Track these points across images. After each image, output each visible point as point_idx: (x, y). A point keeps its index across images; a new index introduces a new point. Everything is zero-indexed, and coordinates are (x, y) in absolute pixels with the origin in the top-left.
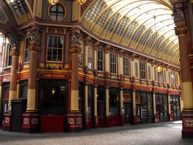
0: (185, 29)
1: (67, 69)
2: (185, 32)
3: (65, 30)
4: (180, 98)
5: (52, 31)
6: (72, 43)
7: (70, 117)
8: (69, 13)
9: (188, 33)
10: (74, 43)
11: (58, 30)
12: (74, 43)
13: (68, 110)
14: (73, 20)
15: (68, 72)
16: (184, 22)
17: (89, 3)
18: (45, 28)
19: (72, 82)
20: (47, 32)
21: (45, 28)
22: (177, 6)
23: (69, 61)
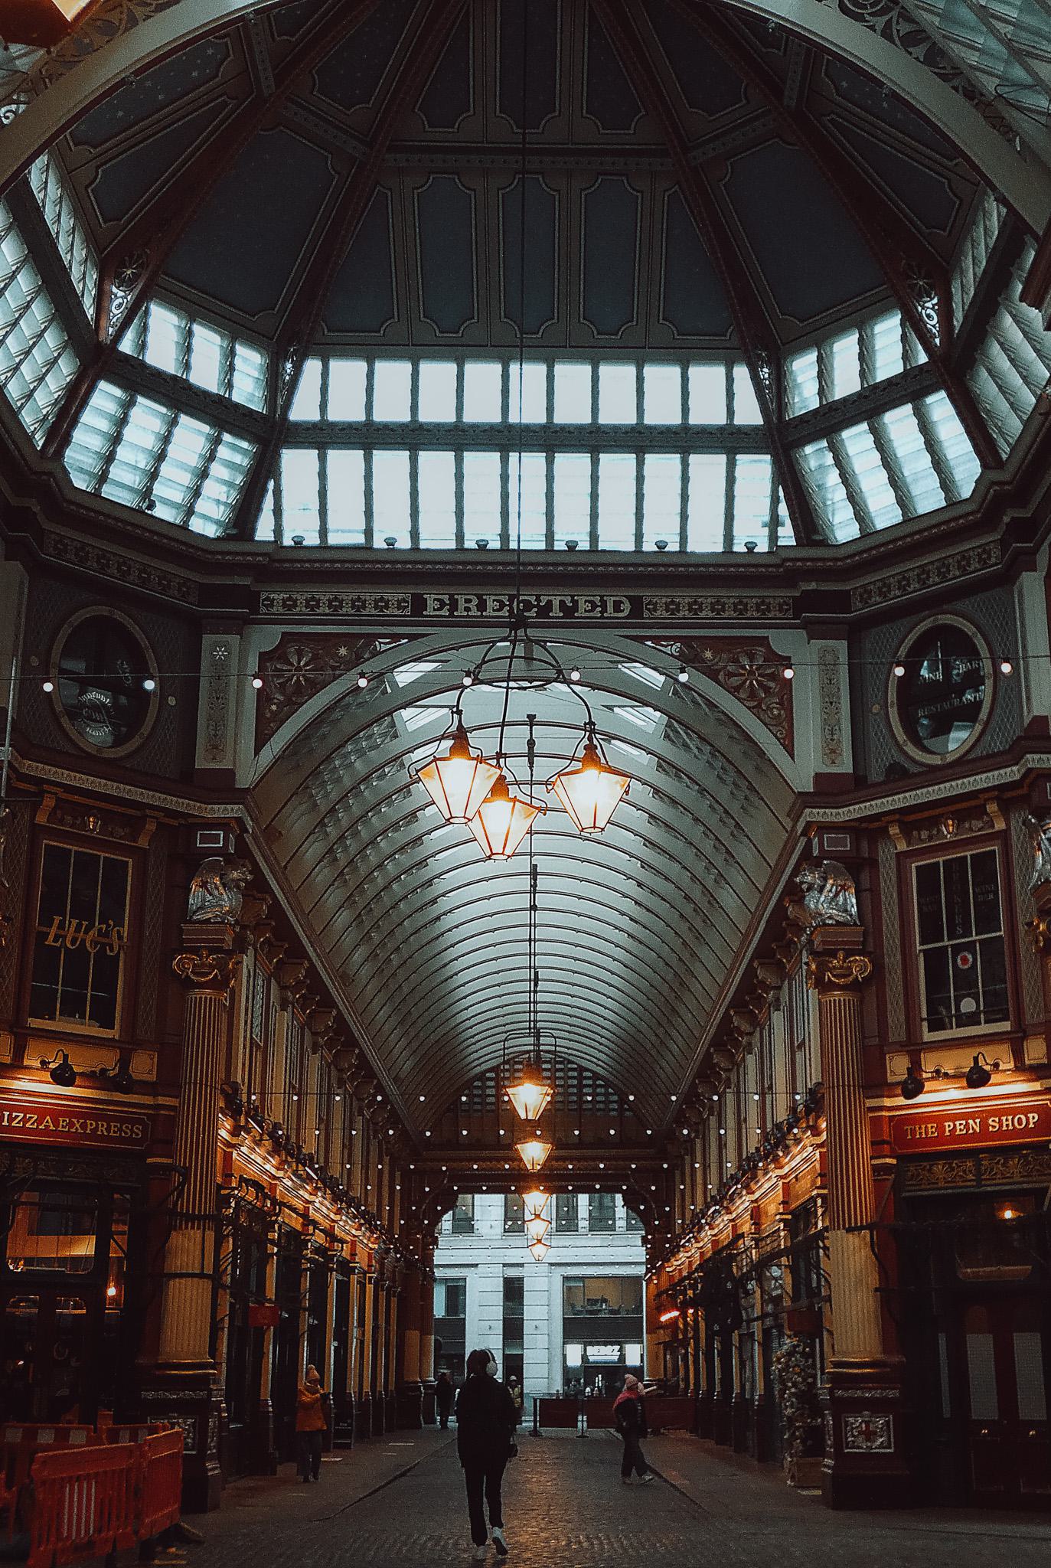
0: (863, 969)
2: (855, 987)
3: (151, 827)
5: (69, 819)
6: (191, 922)
8: (172, 701)
11: (106, 817)
14: (201, 763)
18: (32, 788)
20: (41, 819)
21: (32, 788)
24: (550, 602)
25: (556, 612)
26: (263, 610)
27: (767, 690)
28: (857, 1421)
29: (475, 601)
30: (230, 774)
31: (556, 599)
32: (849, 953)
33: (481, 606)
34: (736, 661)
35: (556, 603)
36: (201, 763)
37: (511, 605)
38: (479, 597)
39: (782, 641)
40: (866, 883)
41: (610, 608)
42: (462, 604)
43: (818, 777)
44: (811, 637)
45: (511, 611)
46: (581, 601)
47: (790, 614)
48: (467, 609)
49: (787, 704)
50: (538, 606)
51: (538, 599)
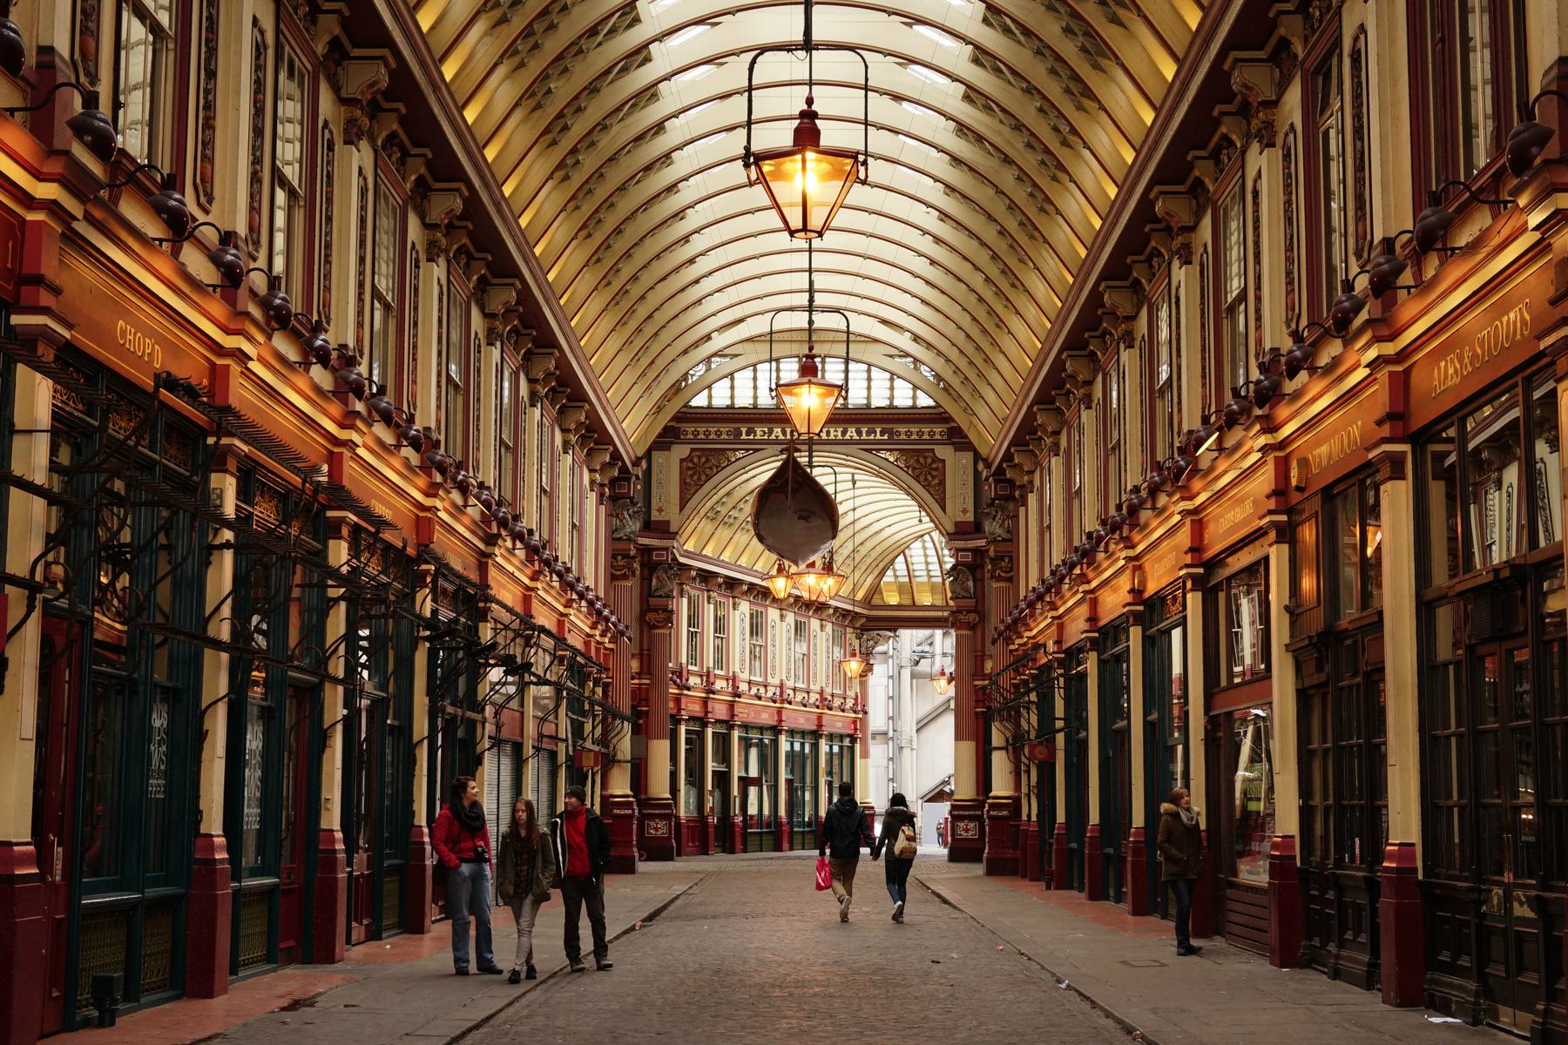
1: (640, 675)
2: (973, 627)
4: (858, 747)
6: (654, 597)
7: (653, 817)
8: (639, 487)
9: (979, 630)
10: (660, 596)
12: (660, 596)
13: (643, 797)
14: (655, 516)
15: (640, 684)
16: (972, 602)
17: (711, 468)
19: (650, 715)
22: (962, 557)
23: (641, 649)
26: (682, 437)
27: (933, 477)
28: (961, 825)
30: (667, 523)
32: (969, 612)
34: (918, 461)
36: (655, 516)
39: (943, 452)
40: (978, 576)
43: (957, 524)
44: (956, 450)
47: (945, 437)
49: (942, 483)
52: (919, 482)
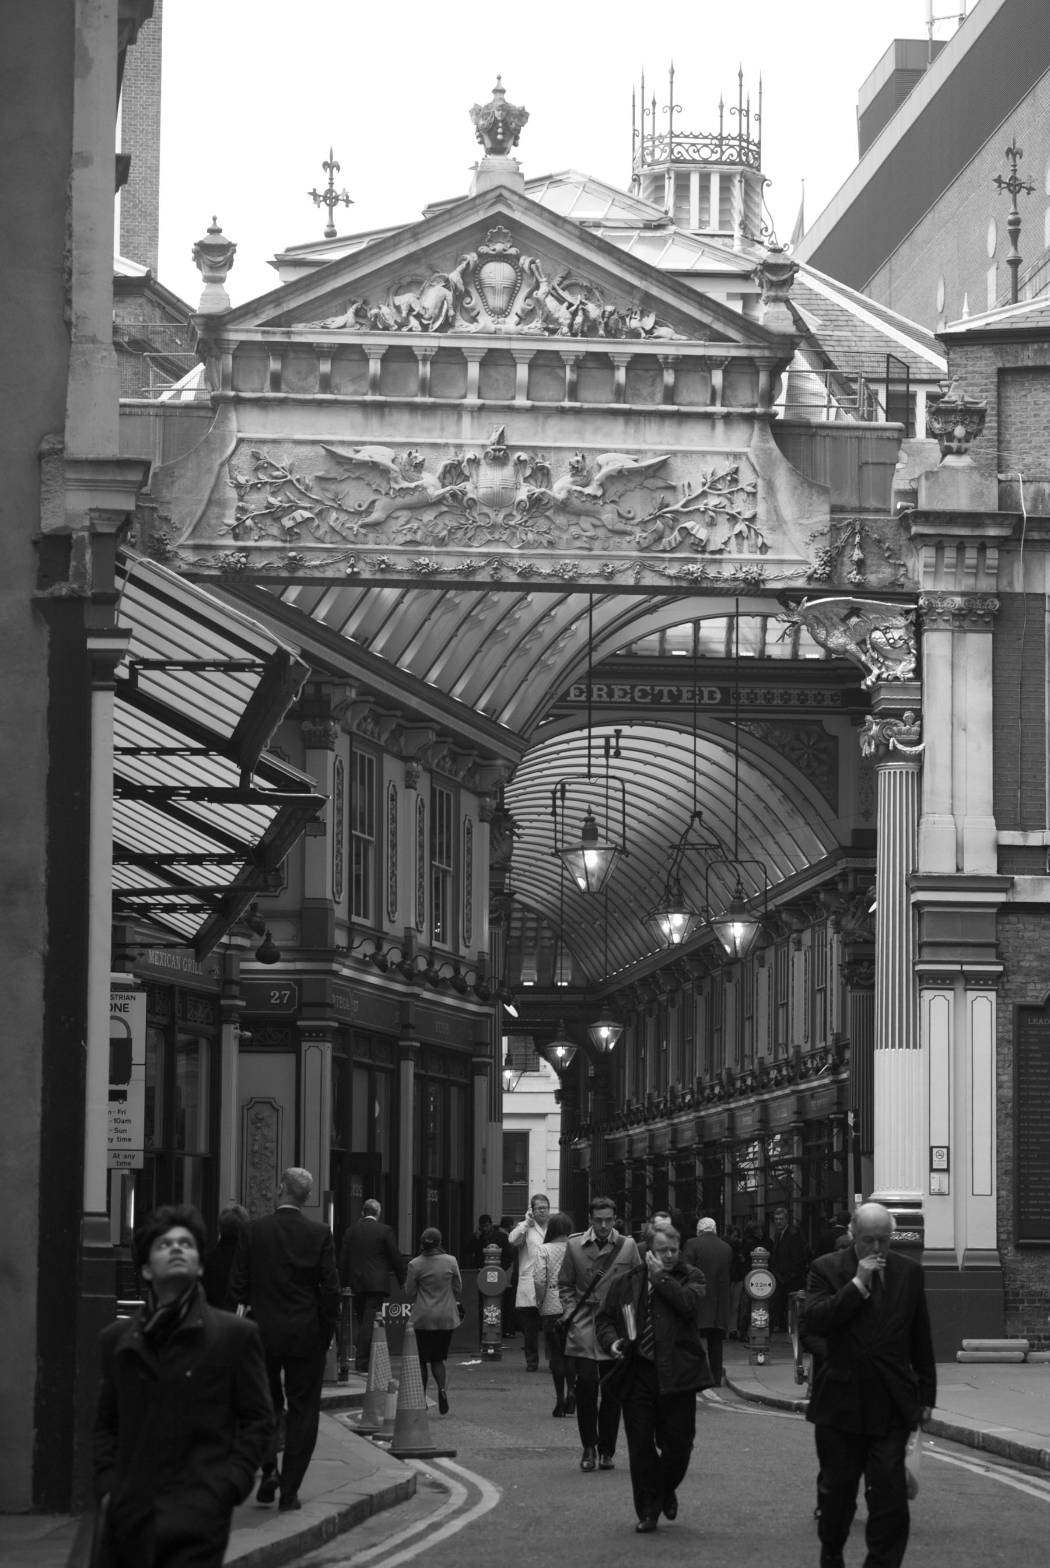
24: (661, 691)
25: (666, 699)
29: (606, 689)
31: (667, 689)
33: (610, 693)
35: (666, 690)
37: (632, 693)
38: (608, 686)
41: (706, 696)
42: (595, 693)
45: (632, 698)
46: (684, 690)
47: (839, 703)
48: (600, 696)
50: (652, 694)
51: (652, 689)
52: (799, 769)
